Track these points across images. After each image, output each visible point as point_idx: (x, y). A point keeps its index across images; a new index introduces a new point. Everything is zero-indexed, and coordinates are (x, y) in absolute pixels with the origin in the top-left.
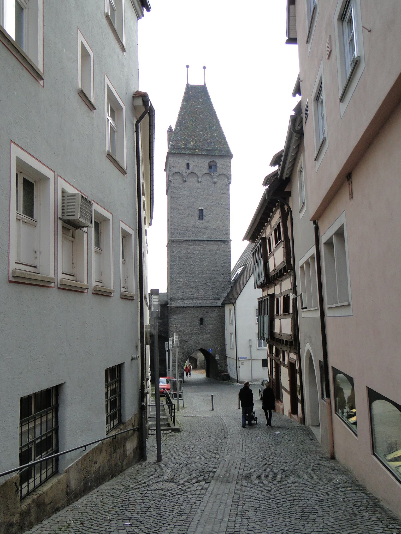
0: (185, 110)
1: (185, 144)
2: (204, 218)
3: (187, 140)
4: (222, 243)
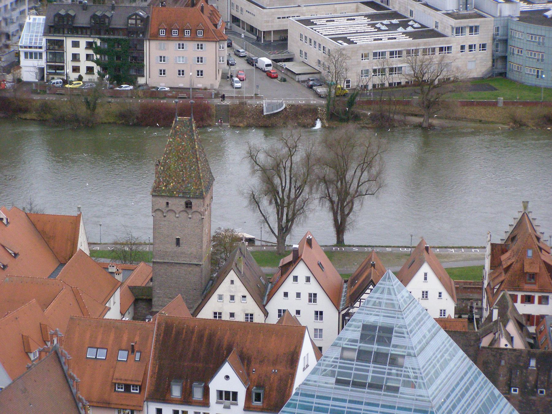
1: (166, 186)
2: (181, 245)
3: (168, 181)
4: (195, 266)
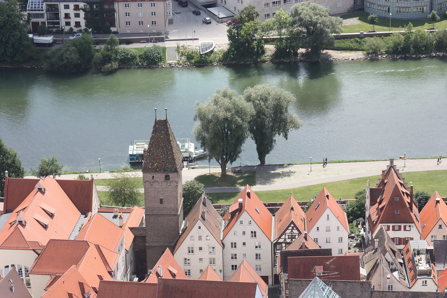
1: (151, 166)
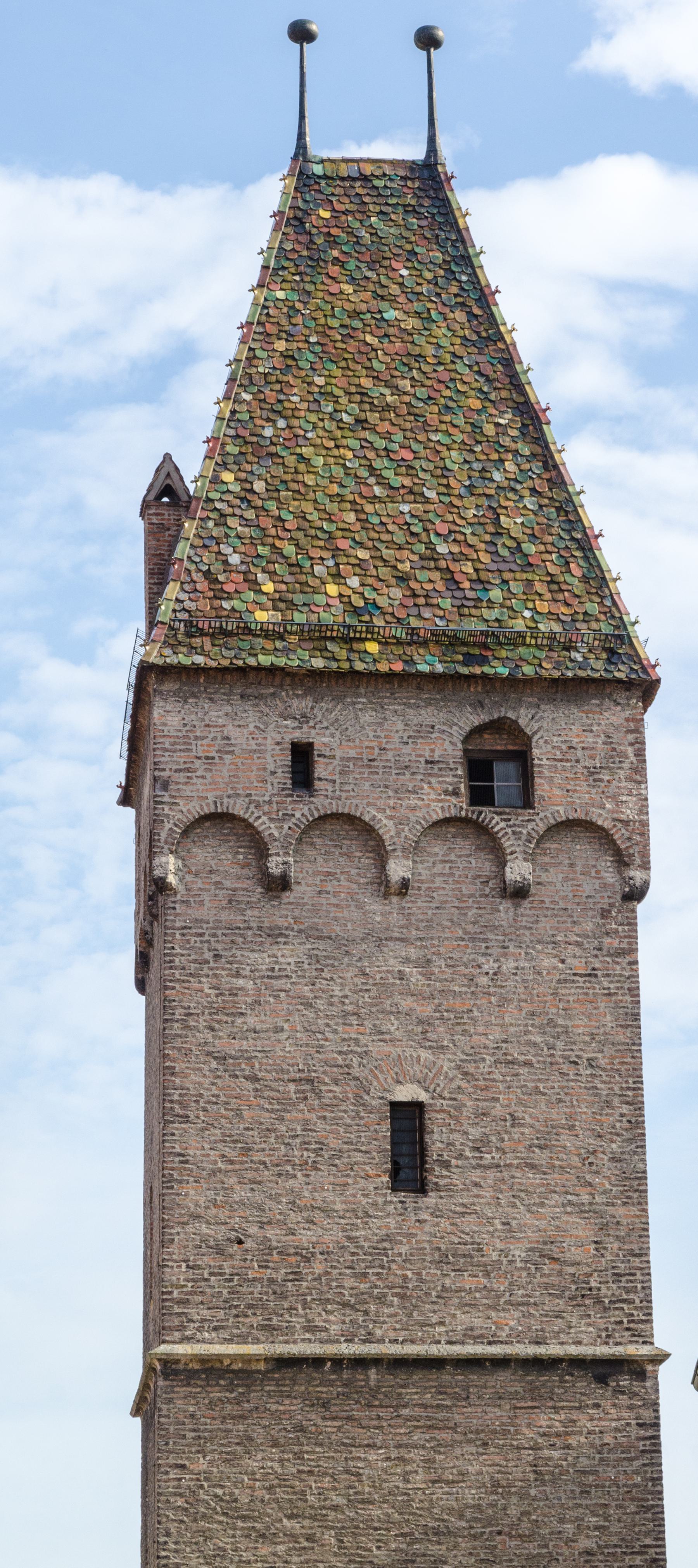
0: (281, 346)
1: (280, 602)
2: (436, 1175)
